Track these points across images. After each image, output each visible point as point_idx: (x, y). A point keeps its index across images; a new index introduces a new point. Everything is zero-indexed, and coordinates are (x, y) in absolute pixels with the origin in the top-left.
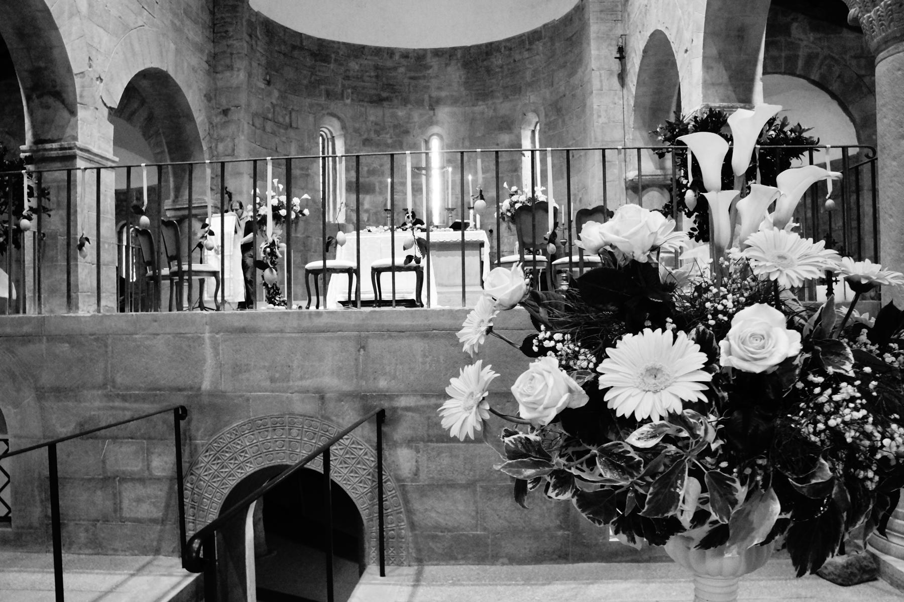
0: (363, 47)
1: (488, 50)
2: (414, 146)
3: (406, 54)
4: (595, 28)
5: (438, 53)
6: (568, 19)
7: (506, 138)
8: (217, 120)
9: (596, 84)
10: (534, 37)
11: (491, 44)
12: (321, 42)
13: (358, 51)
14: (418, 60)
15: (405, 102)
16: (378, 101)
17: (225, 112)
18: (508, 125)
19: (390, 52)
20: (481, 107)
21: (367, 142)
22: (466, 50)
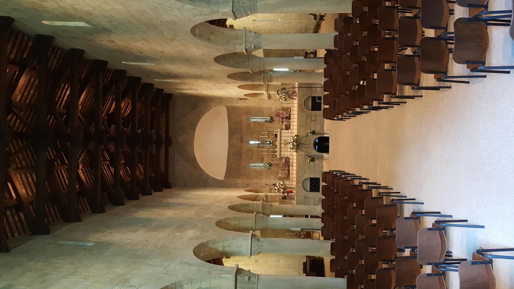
0: (228, 158)
1: (230, 128)
2: (252, 147)
3: (229, 148)
4: (234, 104)
5: (229, 141)
6: (228, 110)
7: (252, 125)
8: (249, 186)
9: (246, 105)
10: (229, 117)
11: (229, 128)
12: (227, 168)
13: (229, 160)
14: (230, 146)
15: (241, 149)
16: (241, 155)
17: (248, 185)
18: (249, 125)
19: (229, 152)
20: (244, 131)
21: (251, 158)
22: (229, 134)
